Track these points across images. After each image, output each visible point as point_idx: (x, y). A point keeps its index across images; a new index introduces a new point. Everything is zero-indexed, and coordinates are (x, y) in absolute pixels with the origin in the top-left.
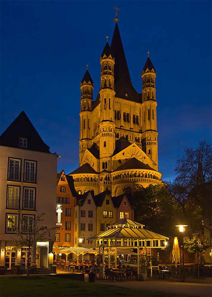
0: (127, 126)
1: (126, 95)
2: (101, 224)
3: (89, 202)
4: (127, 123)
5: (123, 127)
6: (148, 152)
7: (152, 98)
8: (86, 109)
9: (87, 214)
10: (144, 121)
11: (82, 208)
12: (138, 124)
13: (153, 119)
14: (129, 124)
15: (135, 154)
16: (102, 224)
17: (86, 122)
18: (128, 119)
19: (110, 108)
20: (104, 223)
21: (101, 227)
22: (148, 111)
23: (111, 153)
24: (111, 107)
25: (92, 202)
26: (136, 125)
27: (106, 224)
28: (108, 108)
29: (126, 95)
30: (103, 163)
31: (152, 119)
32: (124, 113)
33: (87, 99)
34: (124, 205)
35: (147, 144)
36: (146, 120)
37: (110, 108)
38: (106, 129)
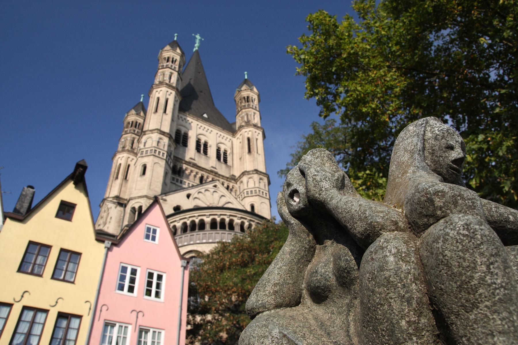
1: (205, 116)
4: (203, 157)
10: (240, 159)
12: (225, 161)
18: (205, 153)
19: (165, 112)
24: (167, 112)
26: (224, 166)
29: (205, 116)
30: (134, 208)
31: (256, 153)
33: (131, 135)
34: (147, 237)
35: (247, 194)
36: (245, 154)
37: (165, 112)
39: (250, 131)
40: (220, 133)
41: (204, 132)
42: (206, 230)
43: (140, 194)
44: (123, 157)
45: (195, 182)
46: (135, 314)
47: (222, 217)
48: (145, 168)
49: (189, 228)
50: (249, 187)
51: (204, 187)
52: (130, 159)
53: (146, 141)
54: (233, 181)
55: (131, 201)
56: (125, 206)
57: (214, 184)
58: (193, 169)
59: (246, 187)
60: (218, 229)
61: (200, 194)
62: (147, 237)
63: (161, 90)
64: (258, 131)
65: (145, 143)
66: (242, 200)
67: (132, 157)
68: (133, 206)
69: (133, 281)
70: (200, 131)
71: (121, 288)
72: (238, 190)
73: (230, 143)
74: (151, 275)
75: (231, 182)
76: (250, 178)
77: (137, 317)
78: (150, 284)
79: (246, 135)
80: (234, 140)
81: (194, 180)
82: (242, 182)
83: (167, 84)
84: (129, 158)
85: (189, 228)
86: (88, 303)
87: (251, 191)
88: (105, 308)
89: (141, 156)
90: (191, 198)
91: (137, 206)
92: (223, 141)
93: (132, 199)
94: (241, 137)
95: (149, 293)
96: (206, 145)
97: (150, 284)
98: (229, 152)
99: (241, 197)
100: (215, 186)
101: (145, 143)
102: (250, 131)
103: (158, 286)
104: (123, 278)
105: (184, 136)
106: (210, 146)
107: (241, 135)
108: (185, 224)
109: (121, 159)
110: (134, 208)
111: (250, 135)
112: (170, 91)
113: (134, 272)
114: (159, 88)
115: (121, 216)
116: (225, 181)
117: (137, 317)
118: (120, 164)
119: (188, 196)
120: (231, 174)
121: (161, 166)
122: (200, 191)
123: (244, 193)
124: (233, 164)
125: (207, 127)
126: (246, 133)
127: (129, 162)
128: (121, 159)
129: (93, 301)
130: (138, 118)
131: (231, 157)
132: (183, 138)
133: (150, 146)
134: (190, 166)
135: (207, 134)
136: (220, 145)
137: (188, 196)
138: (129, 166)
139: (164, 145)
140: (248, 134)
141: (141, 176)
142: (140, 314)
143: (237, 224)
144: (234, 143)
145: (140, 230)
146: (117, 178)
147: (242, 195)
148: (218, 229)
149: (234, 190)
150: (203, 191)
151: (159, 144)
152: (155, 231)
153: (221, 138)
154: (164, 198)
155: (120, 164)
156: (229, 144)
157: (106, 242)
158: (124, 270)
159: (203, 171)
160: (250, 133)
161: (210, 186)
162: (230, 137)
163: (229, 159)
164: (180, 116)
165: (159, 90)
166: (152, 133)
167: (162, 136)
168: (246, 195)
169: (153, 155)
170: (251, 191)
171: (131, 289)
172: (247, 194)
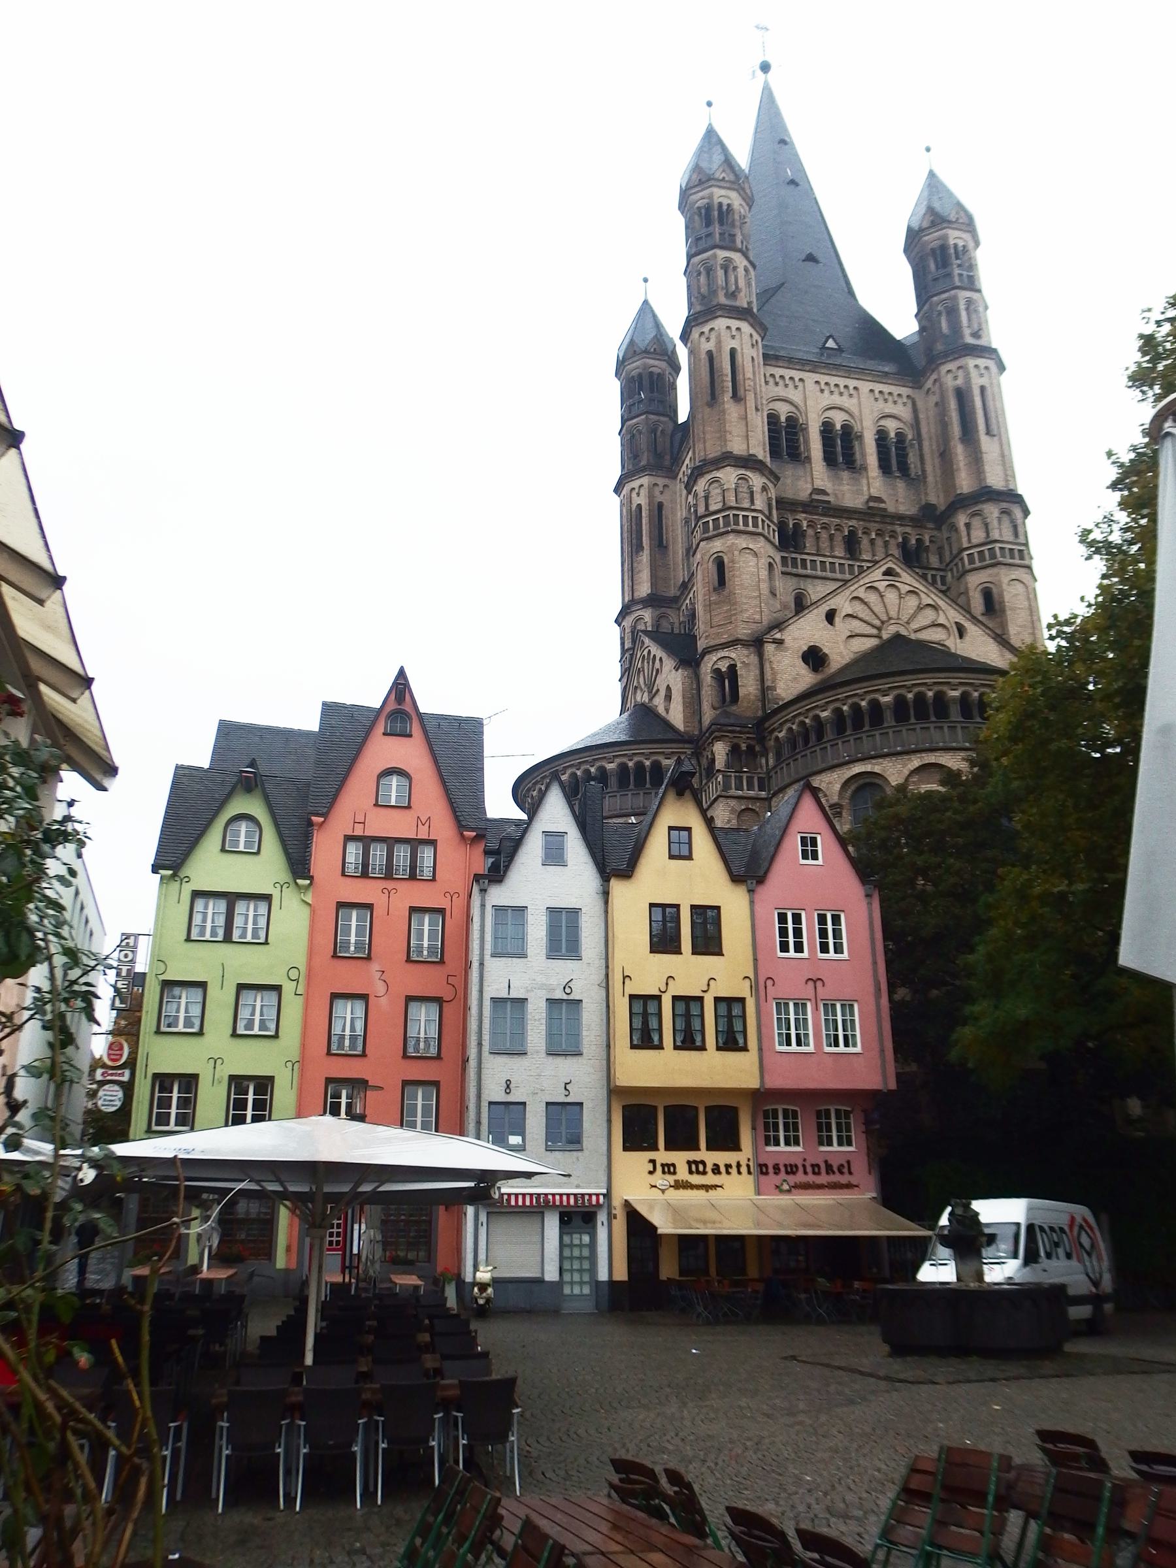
0: (846, 488)
2: (632, 997)
3: (554, 854)
4: (845, 475)
5: (827, 494)
6: (977, 604)
7: (969, 340)
8: (643, 463)
9: (537, 931)
11: (499, 895)
13: (988, 433)
14: (857, 480)
15: (905, 618)
16: (646, 998)
17: (645, 521)
20: (657, 993)
21: (638, 1024)
22: (953, 404)
23: (757, 617)
24: (741, 392)
25: (576, 848)
26: (901, 485)
27: (675, 998)
28: (730, 394)
30: (717, 672)
32: (827, 429)
33: (647, 418)
34: (805, 857)
35: (971, 561)
38: (720, 498)
39: (959, 368)
40: (878, 387)
41: (836, 400)
42: (885, 725)
43: (725, 638)
44: (641, 486)
45: (837, 553)
46: (811, 983)
47: (916, 690)
48: (720, 565)
49: (849, 722)
50: (975, 541)
51: (861, 583)
52: (657, 491)
53: (709, 493)
54: (930, 525)
55: (706, 658)
56: (698, 665)
57: (884, 569)
58: (825, 520)
59: (965, 545)
60: (913, 720)
61: (857, 603)
62: (805, 857)
63: (712, 329)
64: (982, 362)
65: (707, 498)
66: (959, 579)
67: (661, 481)
68: (716, 667)
69: (798, 933)
70: (827, 399)
71: (784, 947)
72: (946, 547)
73: (909, 405)
74: (822, 919)
75: (926, 528)
76: (974, 515)
77: (815, 988)
78: (823, 933)
79: (950, 383)
80: (918, 395)
81: (832, 548)
82: (954, 528)
83: (722, 307)
84: (656, 485)
85: (849, 722)
86: (747, 980)
87: (981, 553)
88: (769, 983)
89: (706, 535)
90: (837, 620)
91: (724, 666)
92: (890, 408)
93: (709, 652)
94: (936, 388)
95: (824, 948)
96: (847, 429)
97: (823, 933)
98: (910, 437)
99: (955, 569)
100: (889, 572)
101: (707, 498)
102: (959, 368)
103: (837, 934)
104: (783, 932)
105: (788, 426)
106: (860, 437)
107: (935, 381)
108: (838, 712)
109: (638, 494)
110: (717, 672)
111: (960, 382)
112: (734, 324)
113: (797, 919)
114: (707, 321)
115: (692, 689)
116: (908, 530)
117: (815, 988)
118: (639, 506)
119: (830, 617)
120: (923, 503)
121: (756, 554)
122: (855, 594)
123: (962, 559)
124: (924, 471)
125: (842, 382)
126: (950, 376)
127: (660, 498)
128: (638, 494)
129: (752, 977)
130: (652, 362)
131: (918, 453)
132: (786, 433)
133: (719, 506)
134: (817, 514)
135: (845, 401)
136: (882, 422)
137: (830, 617)
138: (660, 506)
139: (752, 493)
140: (956, 378)
141: (715, 589)
142: (819, 984)
143: (954, 699)
144: (920, 404)
145: (793, 843)
146: (640, 547)
147: (956, 565)
148: (913, 720)
149: (933, 548)
150: (861, 593)
151: (740, 496)
152: (814, 842)
153: (881, 401)
154: (778, 636)
155: (639, 506)
156: (904, 412)
157: (749, 882)
158: (782, 918)
159: (850, 519)
160: (960, 373)
161: (877, 574)
162: (905, 391)
163: (912, 459)
164: (768, 375)
165: (706, 329)
166: (718, 469)
167: (742, 471)
168: (968, 567)
169: (733, 531)
170: (981, 553)
171: (799, 948)
172: (971, 561)
